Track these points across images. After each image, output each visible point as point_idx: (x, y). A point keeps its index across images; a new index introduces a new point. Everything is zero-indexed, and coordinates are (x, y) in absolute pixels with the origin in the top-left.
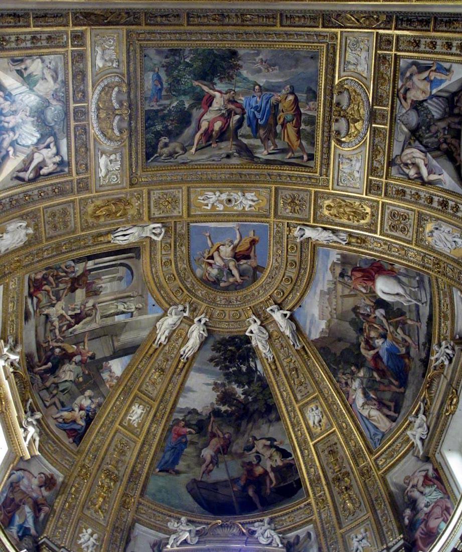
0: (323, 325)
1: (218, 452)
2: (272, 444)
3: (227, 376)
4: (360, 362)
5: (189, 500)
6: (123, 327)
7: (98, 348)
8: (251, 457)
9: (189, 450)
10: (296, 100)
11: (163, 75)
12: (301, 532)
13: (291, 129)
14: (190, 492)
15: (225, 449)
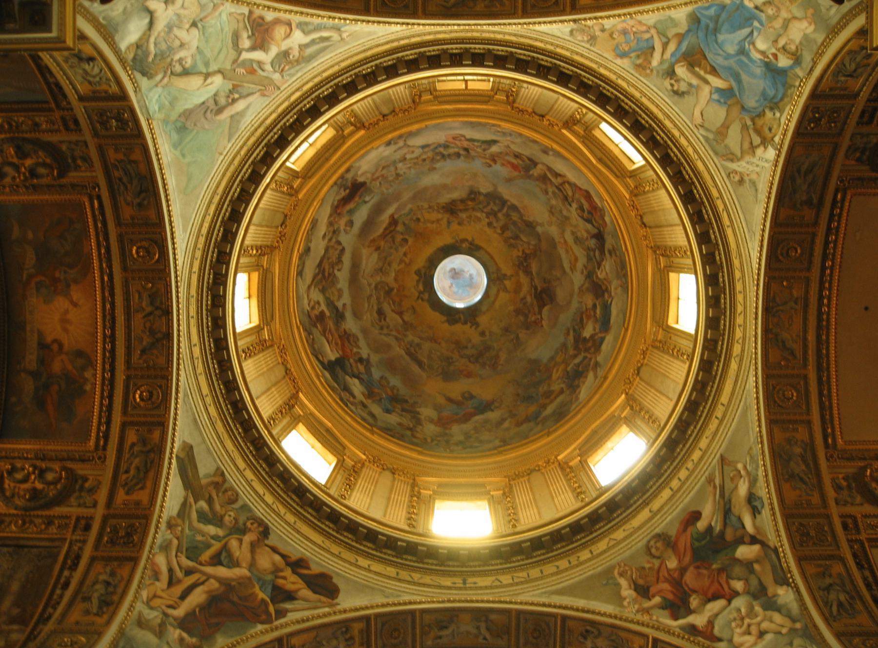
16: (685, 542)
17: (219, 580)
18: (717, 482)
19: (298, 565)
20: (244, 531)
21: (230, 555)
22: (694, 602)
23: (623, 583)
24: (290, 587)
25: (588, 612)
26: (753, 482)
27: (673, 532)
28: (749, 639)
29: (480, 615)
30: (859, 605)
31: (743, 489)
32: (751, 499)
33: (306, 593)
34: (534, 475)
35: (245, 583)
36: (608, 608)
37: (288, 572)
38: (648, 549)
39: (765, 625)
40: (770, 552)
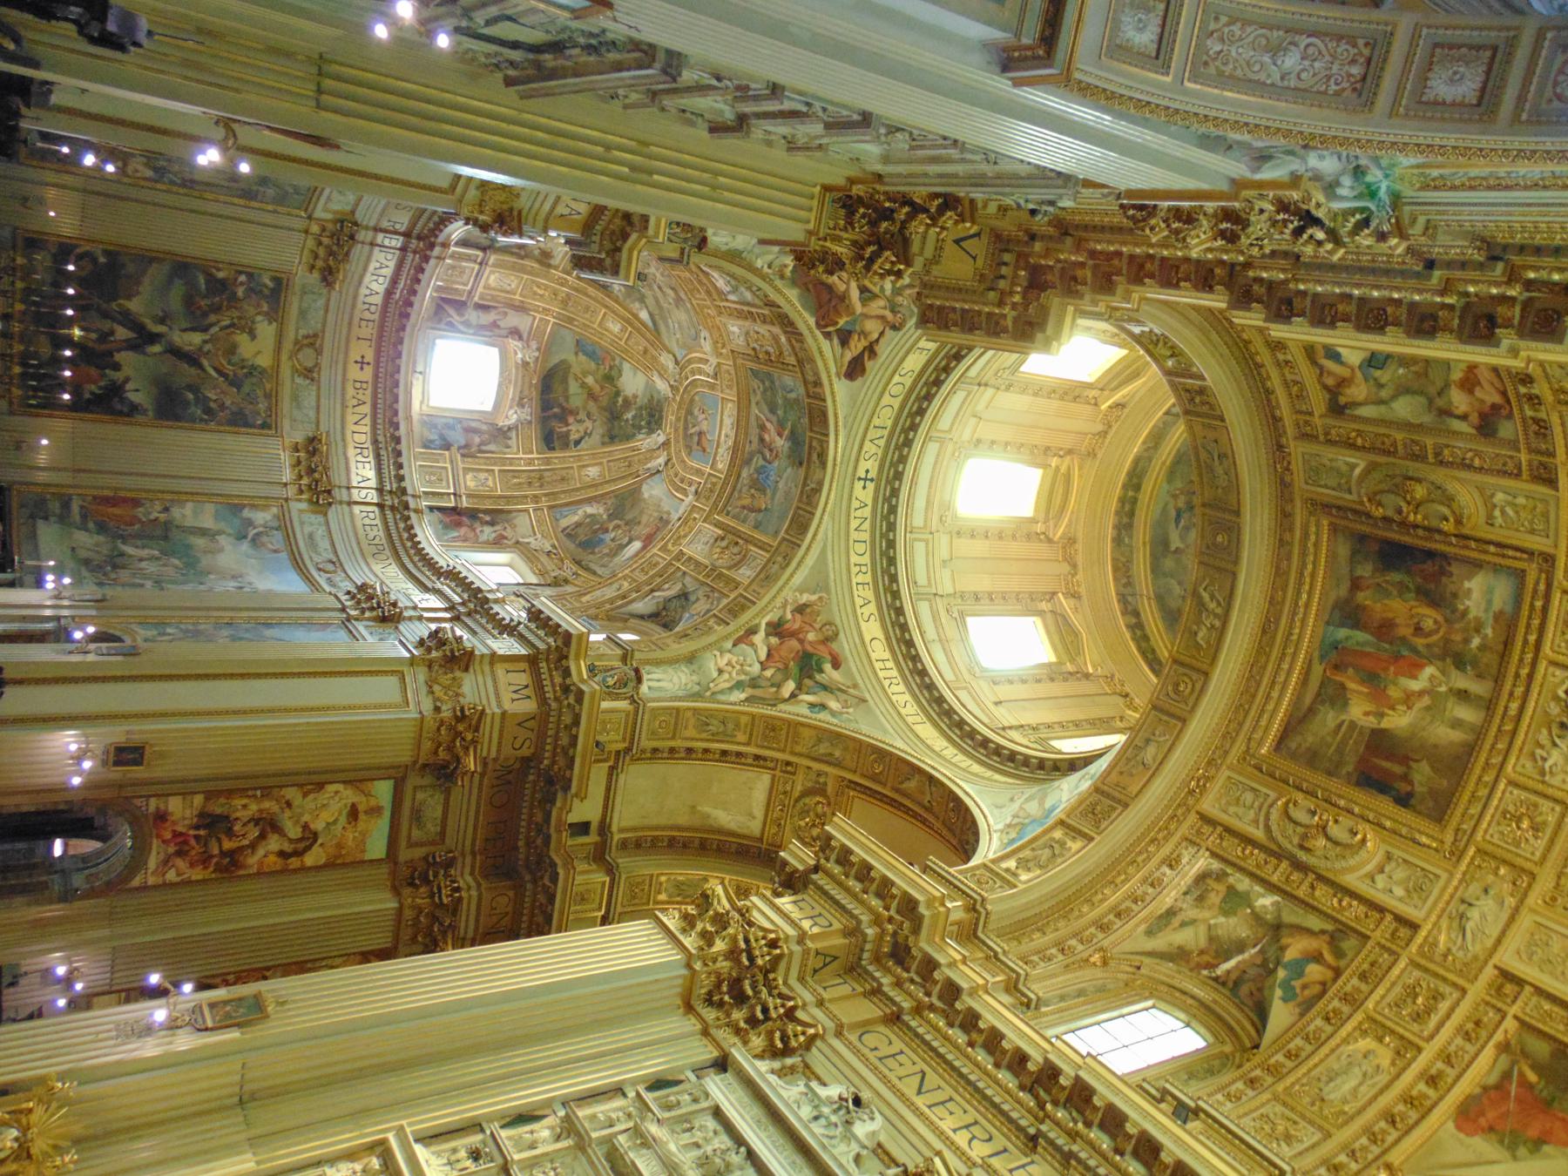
0: (646, 495)
1: (590, 389)
2: (587, 434)
3: (641, 408)
4: (611, 517)
5: (555, 360)
6: (667, 326)
7: (650, 301)
8: (582, 416)
9: (593, 365)
10: (760, 511)
11: (793, 395)
12: (513, 442)
13: (746, 502)
14: (563, 362)
15: (592, 396)
16: (822, 651)
17: (847, 289)
18: (851, 691)
19: (871, 350)
20: (893, 311)
21: (870, 299)
22: (774, 640)
23: (814, 598)
24: (852, 344)
25: (799, 565)
26: (833, 713)
27: (834, 646)
28: (722, 662)
29: (821, 483)
30: (704, 735)
31: (834, 705)
32: (823, 707)
33: (848, 356)
34: (1066, 568)
35: (850, 310)
36: (798, 579)
37: (864, 343)
38: (830, 624)
39: (726, 676)
40: (776, 701)
